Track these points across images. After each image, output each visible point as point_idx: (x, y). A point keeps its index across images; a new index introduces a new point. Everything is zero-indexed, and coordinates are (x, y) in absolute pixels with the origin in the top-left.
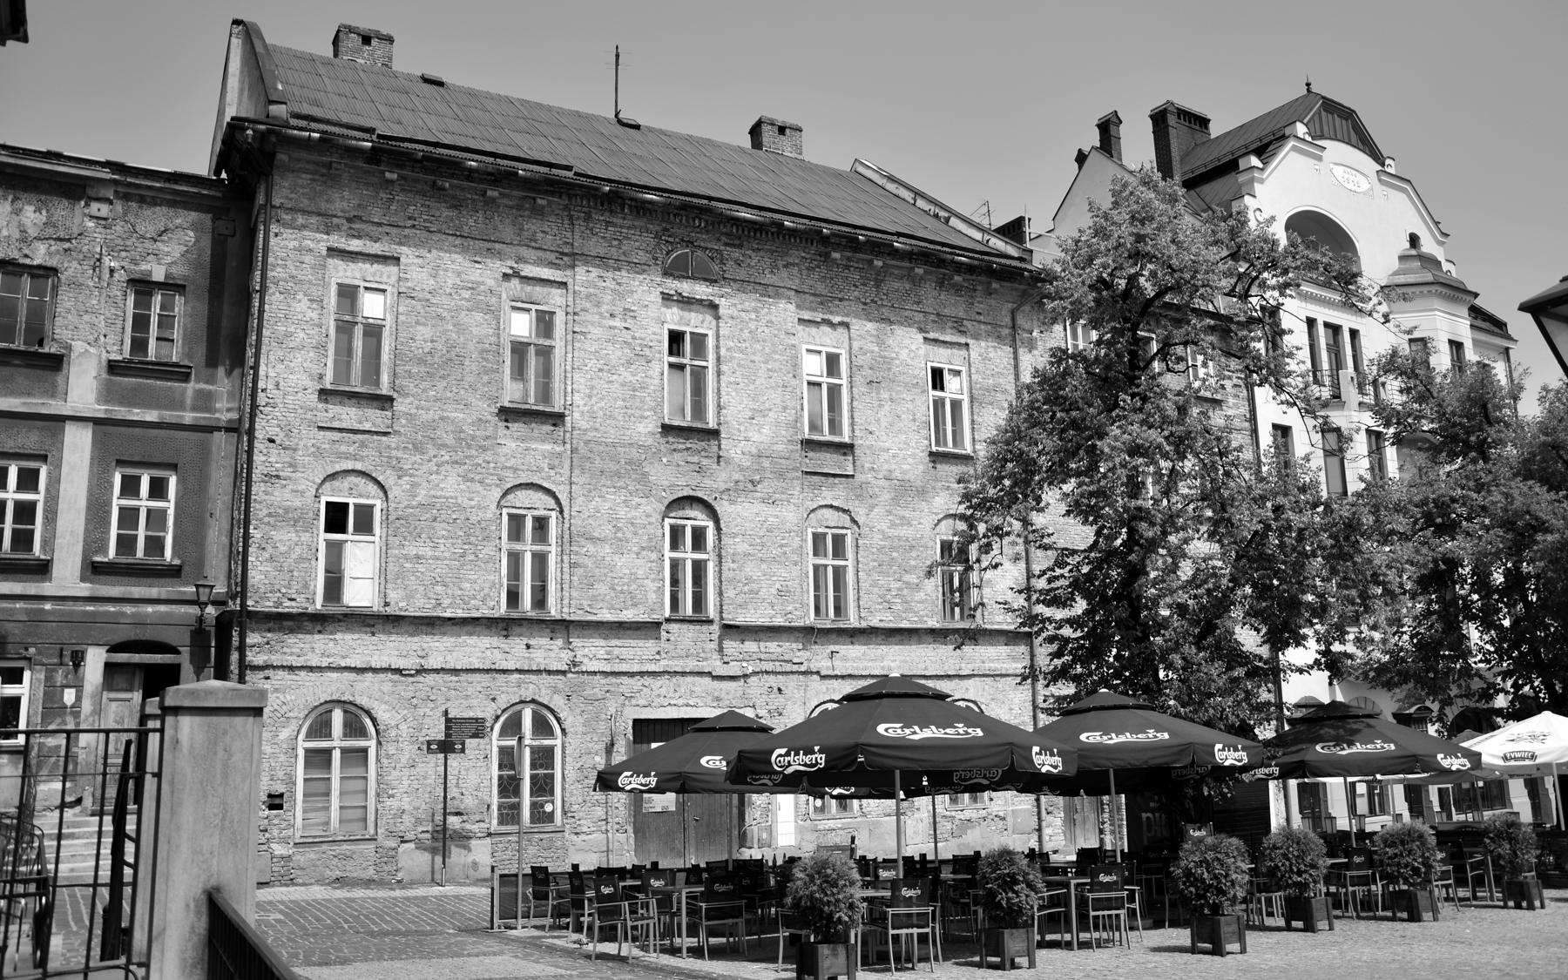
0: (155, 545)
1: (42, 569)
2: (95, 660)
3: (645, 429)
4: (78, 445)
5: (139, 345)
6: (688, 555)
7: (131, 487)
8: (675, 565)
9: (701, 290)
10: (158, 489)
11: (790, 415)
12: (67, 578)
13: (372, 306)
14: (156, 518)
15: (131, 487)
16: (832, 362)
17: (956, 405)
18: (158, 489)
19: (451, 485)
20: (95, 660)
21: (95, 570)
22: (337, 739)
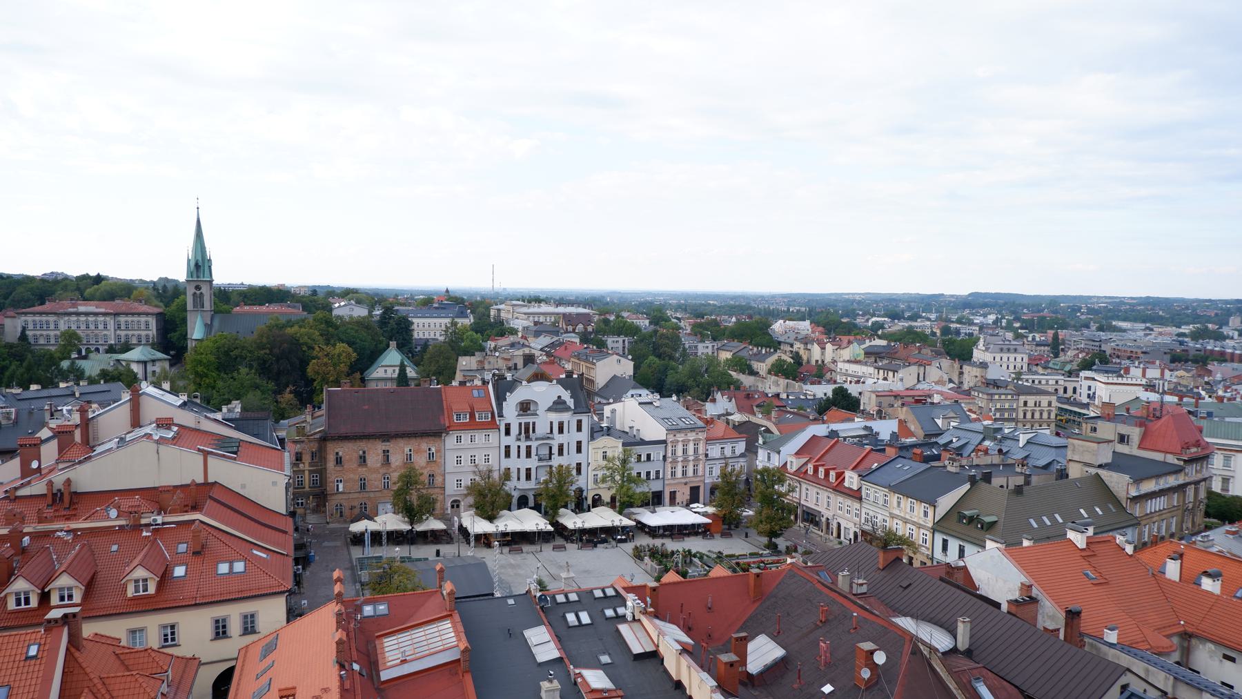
0: (317, 483)
1: (304, 488)
2: (311, 497)
3: (379, 465)
4: (307, 473)
5: (313, 459)
6: (386, 481)
7: (313, 477)
8: (384, 483)
9: (388, 444)
10: (317, 476)
11: (402, 460)
12: (307, 489)
13: (340, 454)
14: (317, 480)
15: (313, 477)
16: (410, 450)
17: (433, 453)
18: (317, 476)
19: (352, 476)
20: (311, 497)
21: (309, 487)
22: (339, 507)
